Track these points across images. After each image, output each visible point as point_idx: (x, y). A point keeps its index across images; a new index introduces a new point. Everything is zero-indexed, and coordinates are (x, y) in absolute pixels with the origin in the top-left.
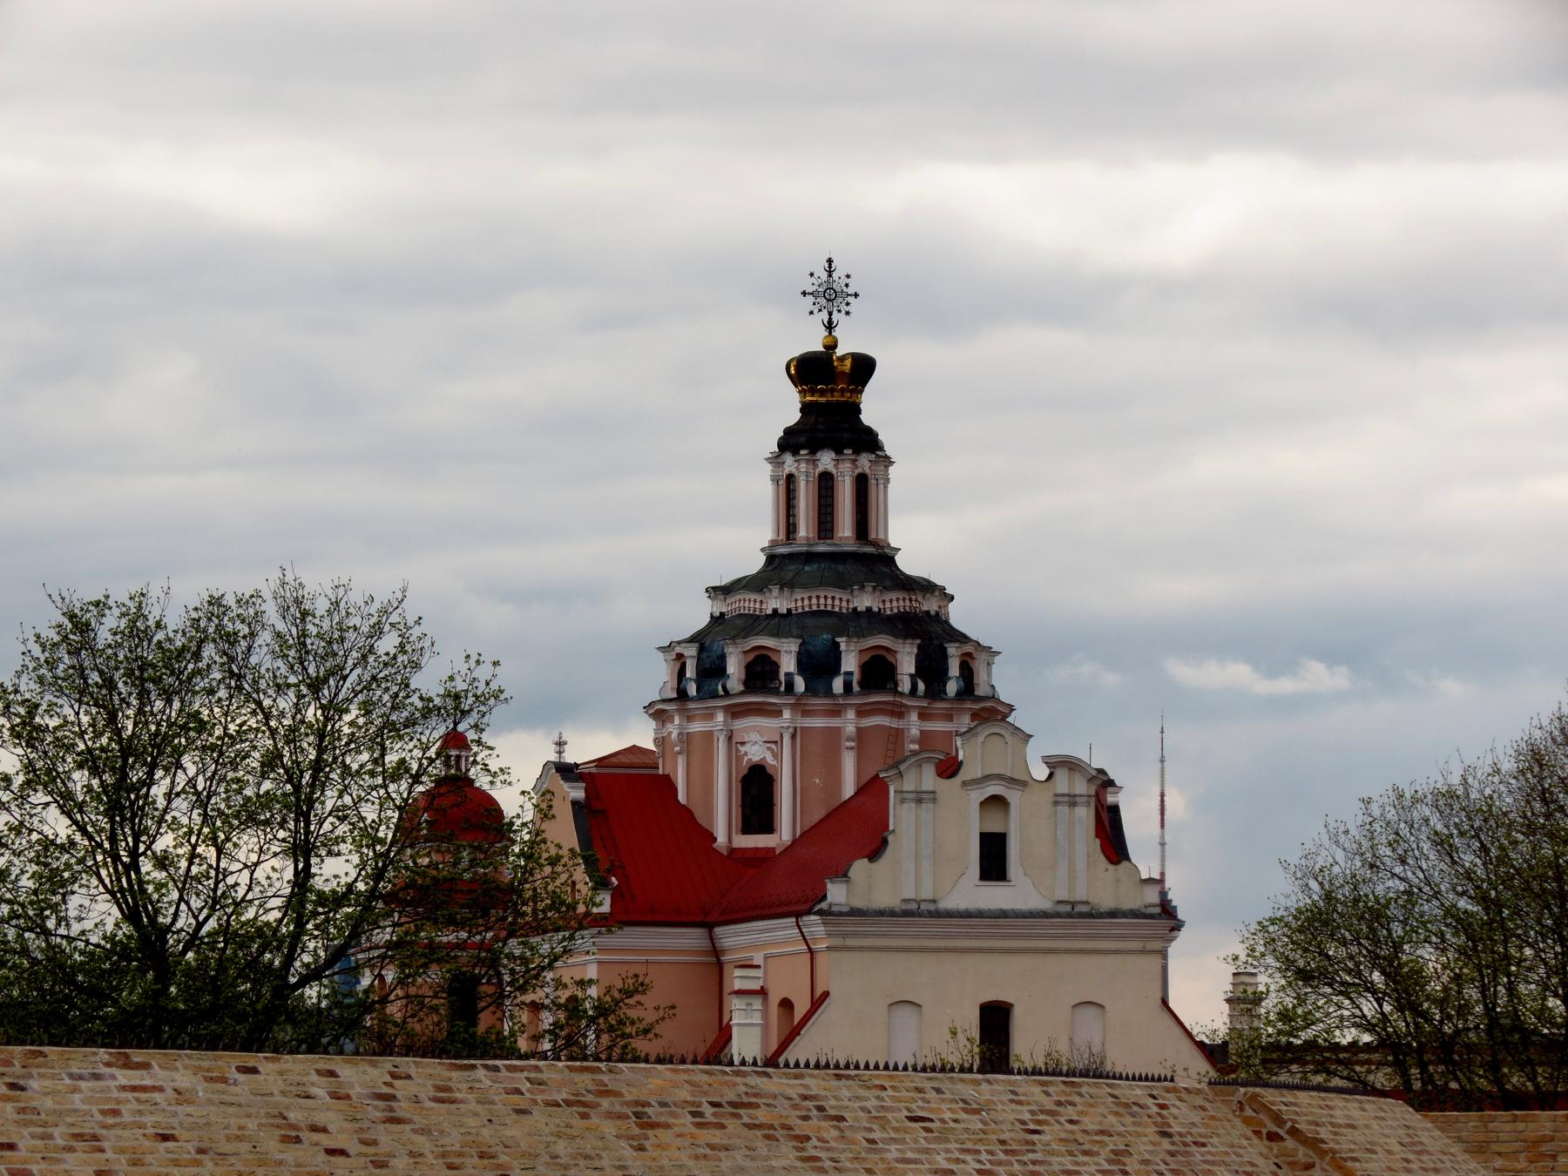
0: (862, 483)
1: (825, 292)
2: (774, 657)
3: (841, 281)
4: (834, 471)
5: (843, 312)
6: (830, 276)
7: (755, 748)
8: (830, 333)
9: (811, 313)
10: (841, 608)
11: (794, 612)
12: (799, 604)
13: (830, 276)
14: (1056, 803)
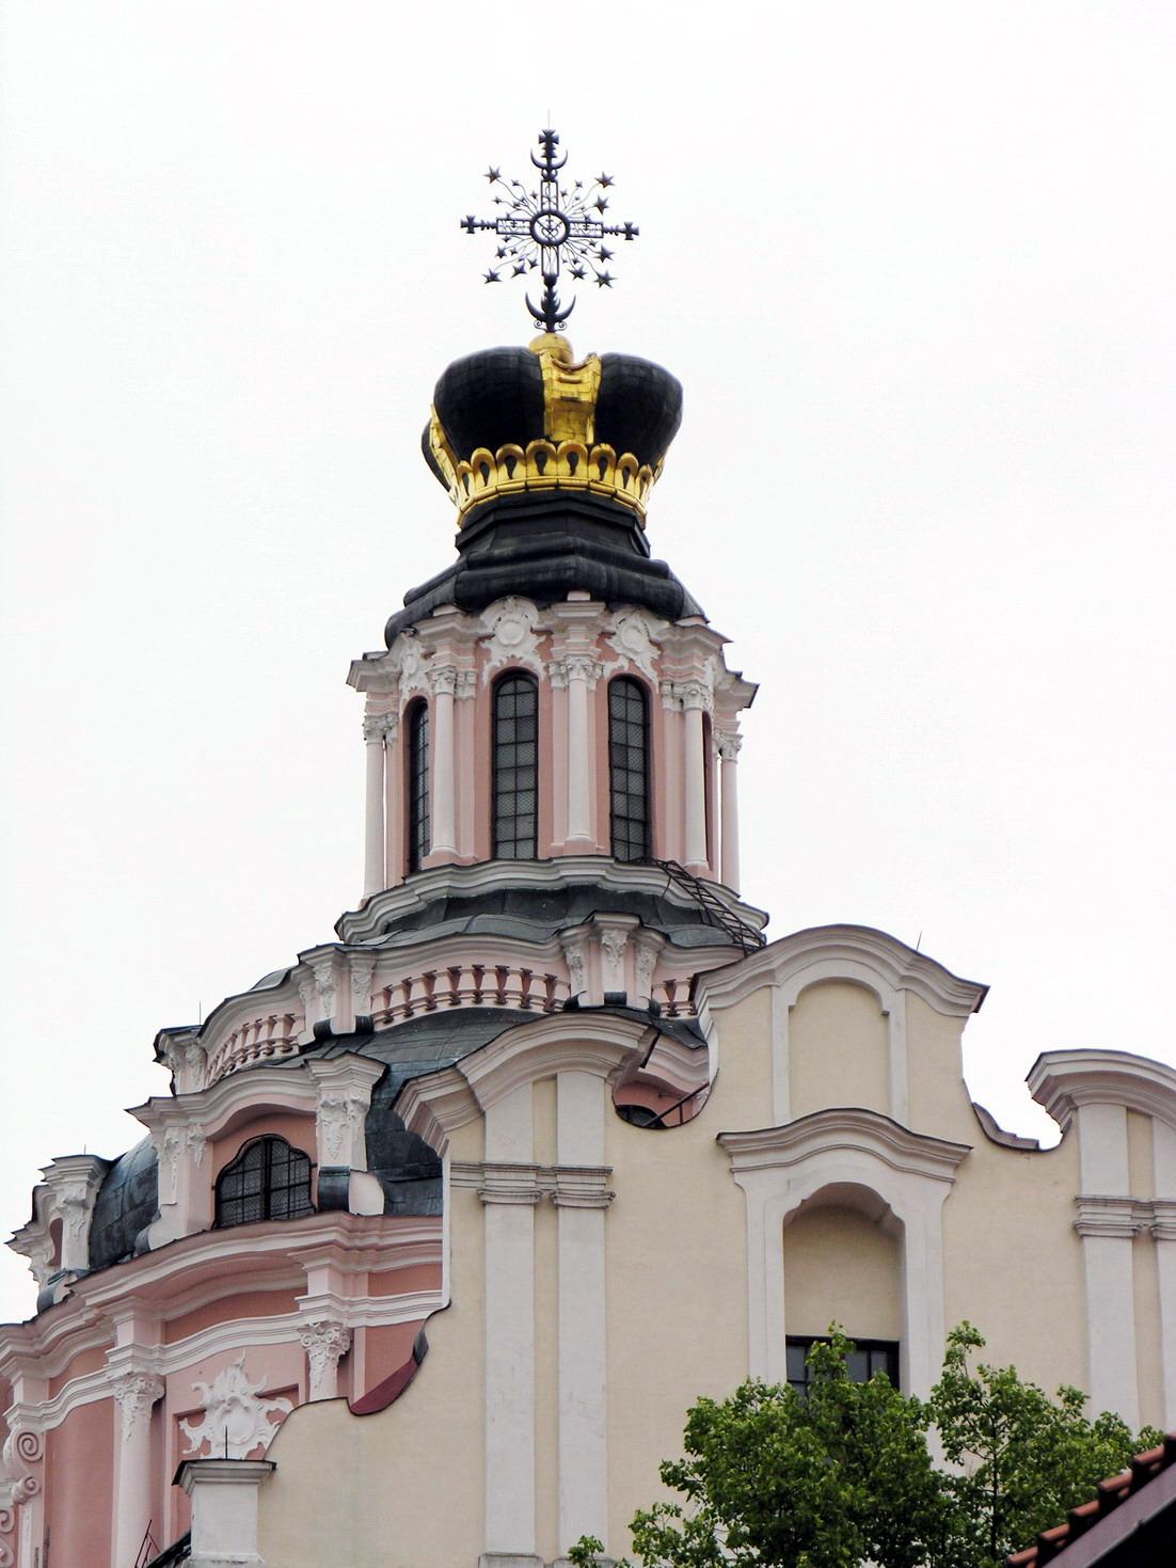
0: (629, 690)
1: (533, 222)
2: (295, 1137)
3: (581, 193)
4: (537, 665)
5: (591, 277)
6: (549, 179)
7: (236, 1419)
8: (550, 330)
9: (493, 278)
10: (526, 1000)
11: (379, 1027)
12: (398, 999)
13: (549, 179)
14: (1079, 1231)
